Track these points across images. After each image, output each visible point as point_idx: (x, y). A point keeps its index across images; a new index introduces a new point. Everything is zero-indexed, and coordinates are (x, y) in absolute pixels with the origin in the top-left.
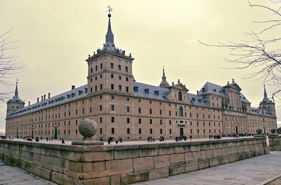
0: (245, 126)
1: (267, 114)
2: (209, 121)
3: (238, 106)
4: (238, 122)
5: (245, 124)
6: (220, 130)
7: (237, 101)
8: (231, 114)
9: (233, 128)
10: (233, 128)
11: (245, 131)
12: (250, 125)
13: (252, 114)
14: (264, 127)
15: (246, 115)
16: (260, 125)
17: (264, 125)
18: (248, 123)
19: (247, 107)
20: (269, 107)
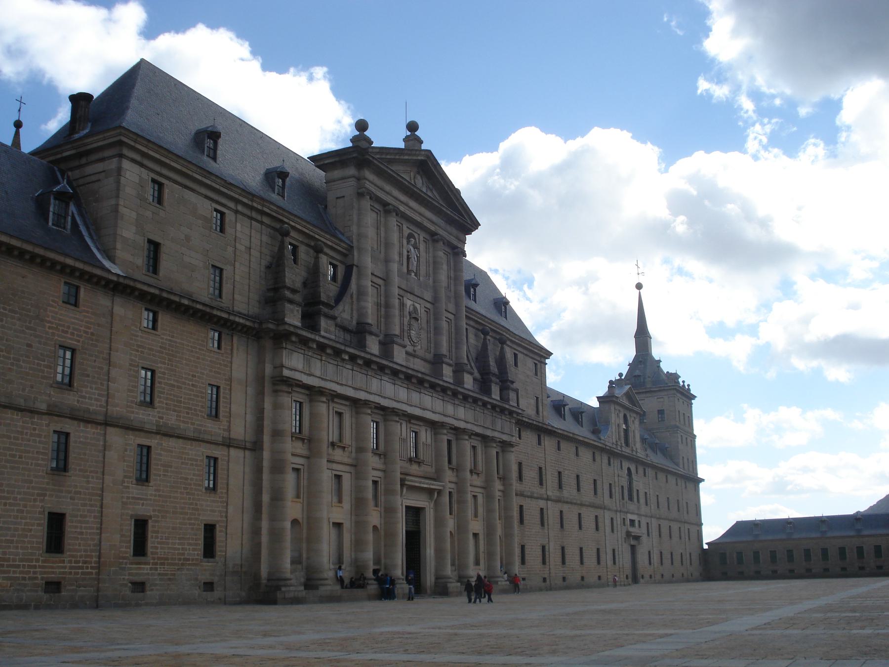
0: (489, 511)
1: (649, 452)
2: (53, 412)
3: (437, 345)
4: (430, 470)
5: (489, 497)
6: (210, 530)
7: (435, 301)
8: (362, 396)
9: (374, 518)
10: (374, 518)
11: (490, 555)
12: (532, 508)
13: (551, 432)
14: (628, 534)
15: (502, 429)
16: (608, 515)
17: (632, 522)
18: (520, 494)
19: (520, 374)
20: (661, 412)
